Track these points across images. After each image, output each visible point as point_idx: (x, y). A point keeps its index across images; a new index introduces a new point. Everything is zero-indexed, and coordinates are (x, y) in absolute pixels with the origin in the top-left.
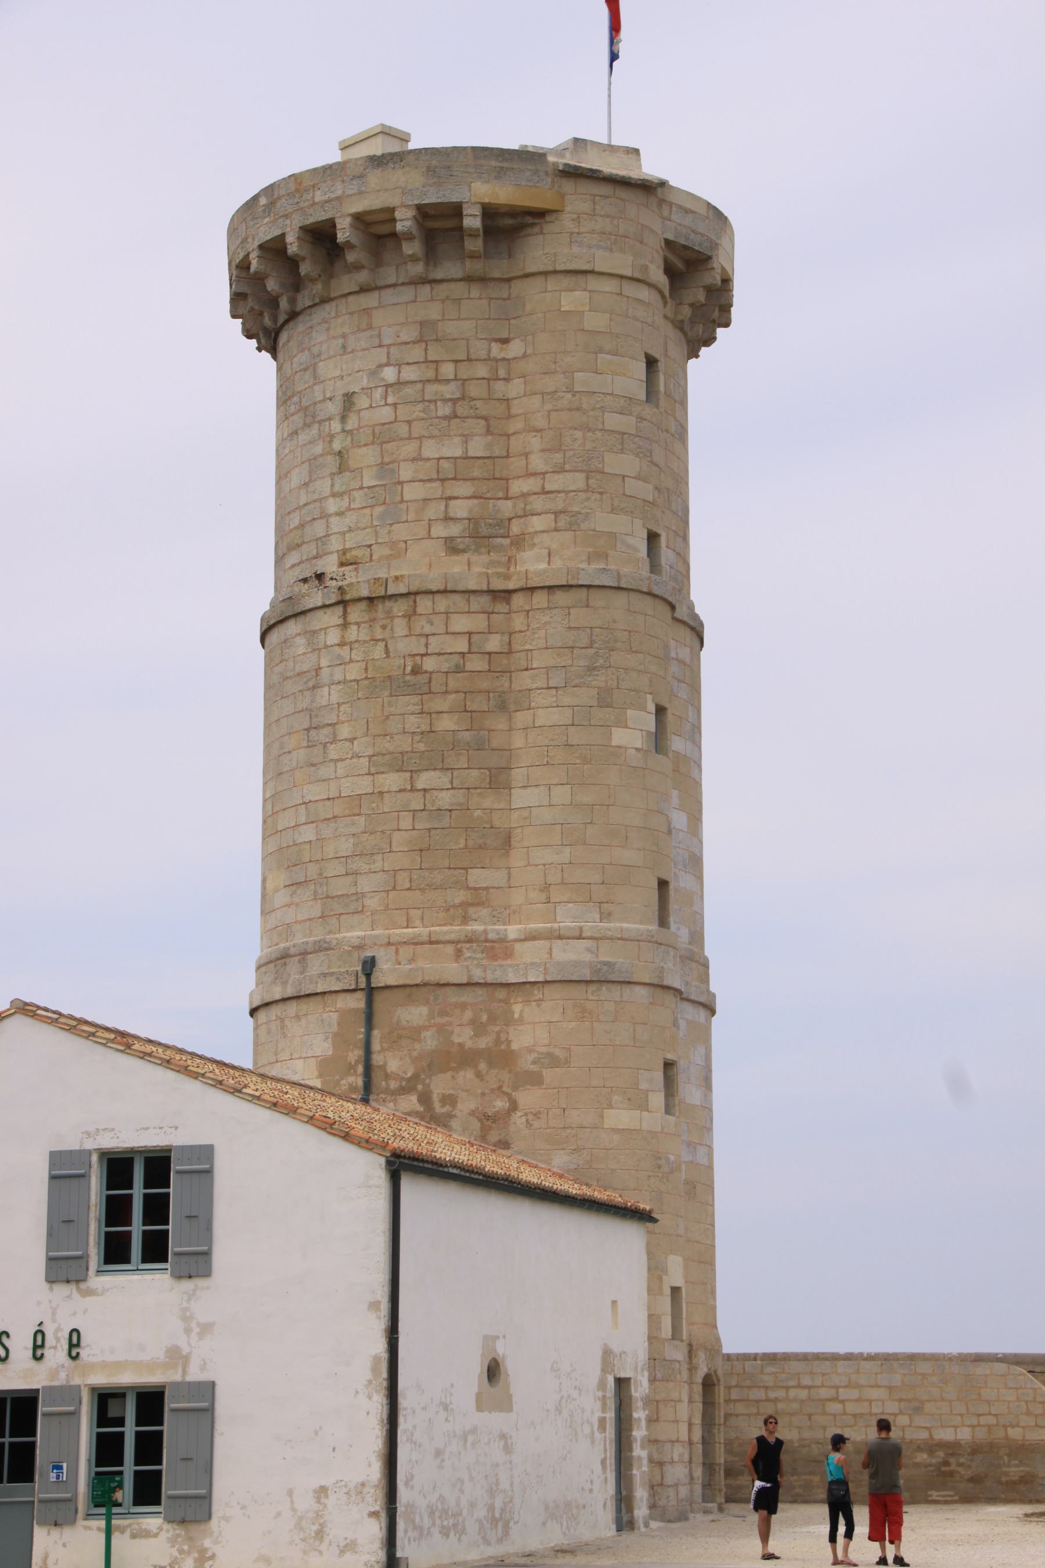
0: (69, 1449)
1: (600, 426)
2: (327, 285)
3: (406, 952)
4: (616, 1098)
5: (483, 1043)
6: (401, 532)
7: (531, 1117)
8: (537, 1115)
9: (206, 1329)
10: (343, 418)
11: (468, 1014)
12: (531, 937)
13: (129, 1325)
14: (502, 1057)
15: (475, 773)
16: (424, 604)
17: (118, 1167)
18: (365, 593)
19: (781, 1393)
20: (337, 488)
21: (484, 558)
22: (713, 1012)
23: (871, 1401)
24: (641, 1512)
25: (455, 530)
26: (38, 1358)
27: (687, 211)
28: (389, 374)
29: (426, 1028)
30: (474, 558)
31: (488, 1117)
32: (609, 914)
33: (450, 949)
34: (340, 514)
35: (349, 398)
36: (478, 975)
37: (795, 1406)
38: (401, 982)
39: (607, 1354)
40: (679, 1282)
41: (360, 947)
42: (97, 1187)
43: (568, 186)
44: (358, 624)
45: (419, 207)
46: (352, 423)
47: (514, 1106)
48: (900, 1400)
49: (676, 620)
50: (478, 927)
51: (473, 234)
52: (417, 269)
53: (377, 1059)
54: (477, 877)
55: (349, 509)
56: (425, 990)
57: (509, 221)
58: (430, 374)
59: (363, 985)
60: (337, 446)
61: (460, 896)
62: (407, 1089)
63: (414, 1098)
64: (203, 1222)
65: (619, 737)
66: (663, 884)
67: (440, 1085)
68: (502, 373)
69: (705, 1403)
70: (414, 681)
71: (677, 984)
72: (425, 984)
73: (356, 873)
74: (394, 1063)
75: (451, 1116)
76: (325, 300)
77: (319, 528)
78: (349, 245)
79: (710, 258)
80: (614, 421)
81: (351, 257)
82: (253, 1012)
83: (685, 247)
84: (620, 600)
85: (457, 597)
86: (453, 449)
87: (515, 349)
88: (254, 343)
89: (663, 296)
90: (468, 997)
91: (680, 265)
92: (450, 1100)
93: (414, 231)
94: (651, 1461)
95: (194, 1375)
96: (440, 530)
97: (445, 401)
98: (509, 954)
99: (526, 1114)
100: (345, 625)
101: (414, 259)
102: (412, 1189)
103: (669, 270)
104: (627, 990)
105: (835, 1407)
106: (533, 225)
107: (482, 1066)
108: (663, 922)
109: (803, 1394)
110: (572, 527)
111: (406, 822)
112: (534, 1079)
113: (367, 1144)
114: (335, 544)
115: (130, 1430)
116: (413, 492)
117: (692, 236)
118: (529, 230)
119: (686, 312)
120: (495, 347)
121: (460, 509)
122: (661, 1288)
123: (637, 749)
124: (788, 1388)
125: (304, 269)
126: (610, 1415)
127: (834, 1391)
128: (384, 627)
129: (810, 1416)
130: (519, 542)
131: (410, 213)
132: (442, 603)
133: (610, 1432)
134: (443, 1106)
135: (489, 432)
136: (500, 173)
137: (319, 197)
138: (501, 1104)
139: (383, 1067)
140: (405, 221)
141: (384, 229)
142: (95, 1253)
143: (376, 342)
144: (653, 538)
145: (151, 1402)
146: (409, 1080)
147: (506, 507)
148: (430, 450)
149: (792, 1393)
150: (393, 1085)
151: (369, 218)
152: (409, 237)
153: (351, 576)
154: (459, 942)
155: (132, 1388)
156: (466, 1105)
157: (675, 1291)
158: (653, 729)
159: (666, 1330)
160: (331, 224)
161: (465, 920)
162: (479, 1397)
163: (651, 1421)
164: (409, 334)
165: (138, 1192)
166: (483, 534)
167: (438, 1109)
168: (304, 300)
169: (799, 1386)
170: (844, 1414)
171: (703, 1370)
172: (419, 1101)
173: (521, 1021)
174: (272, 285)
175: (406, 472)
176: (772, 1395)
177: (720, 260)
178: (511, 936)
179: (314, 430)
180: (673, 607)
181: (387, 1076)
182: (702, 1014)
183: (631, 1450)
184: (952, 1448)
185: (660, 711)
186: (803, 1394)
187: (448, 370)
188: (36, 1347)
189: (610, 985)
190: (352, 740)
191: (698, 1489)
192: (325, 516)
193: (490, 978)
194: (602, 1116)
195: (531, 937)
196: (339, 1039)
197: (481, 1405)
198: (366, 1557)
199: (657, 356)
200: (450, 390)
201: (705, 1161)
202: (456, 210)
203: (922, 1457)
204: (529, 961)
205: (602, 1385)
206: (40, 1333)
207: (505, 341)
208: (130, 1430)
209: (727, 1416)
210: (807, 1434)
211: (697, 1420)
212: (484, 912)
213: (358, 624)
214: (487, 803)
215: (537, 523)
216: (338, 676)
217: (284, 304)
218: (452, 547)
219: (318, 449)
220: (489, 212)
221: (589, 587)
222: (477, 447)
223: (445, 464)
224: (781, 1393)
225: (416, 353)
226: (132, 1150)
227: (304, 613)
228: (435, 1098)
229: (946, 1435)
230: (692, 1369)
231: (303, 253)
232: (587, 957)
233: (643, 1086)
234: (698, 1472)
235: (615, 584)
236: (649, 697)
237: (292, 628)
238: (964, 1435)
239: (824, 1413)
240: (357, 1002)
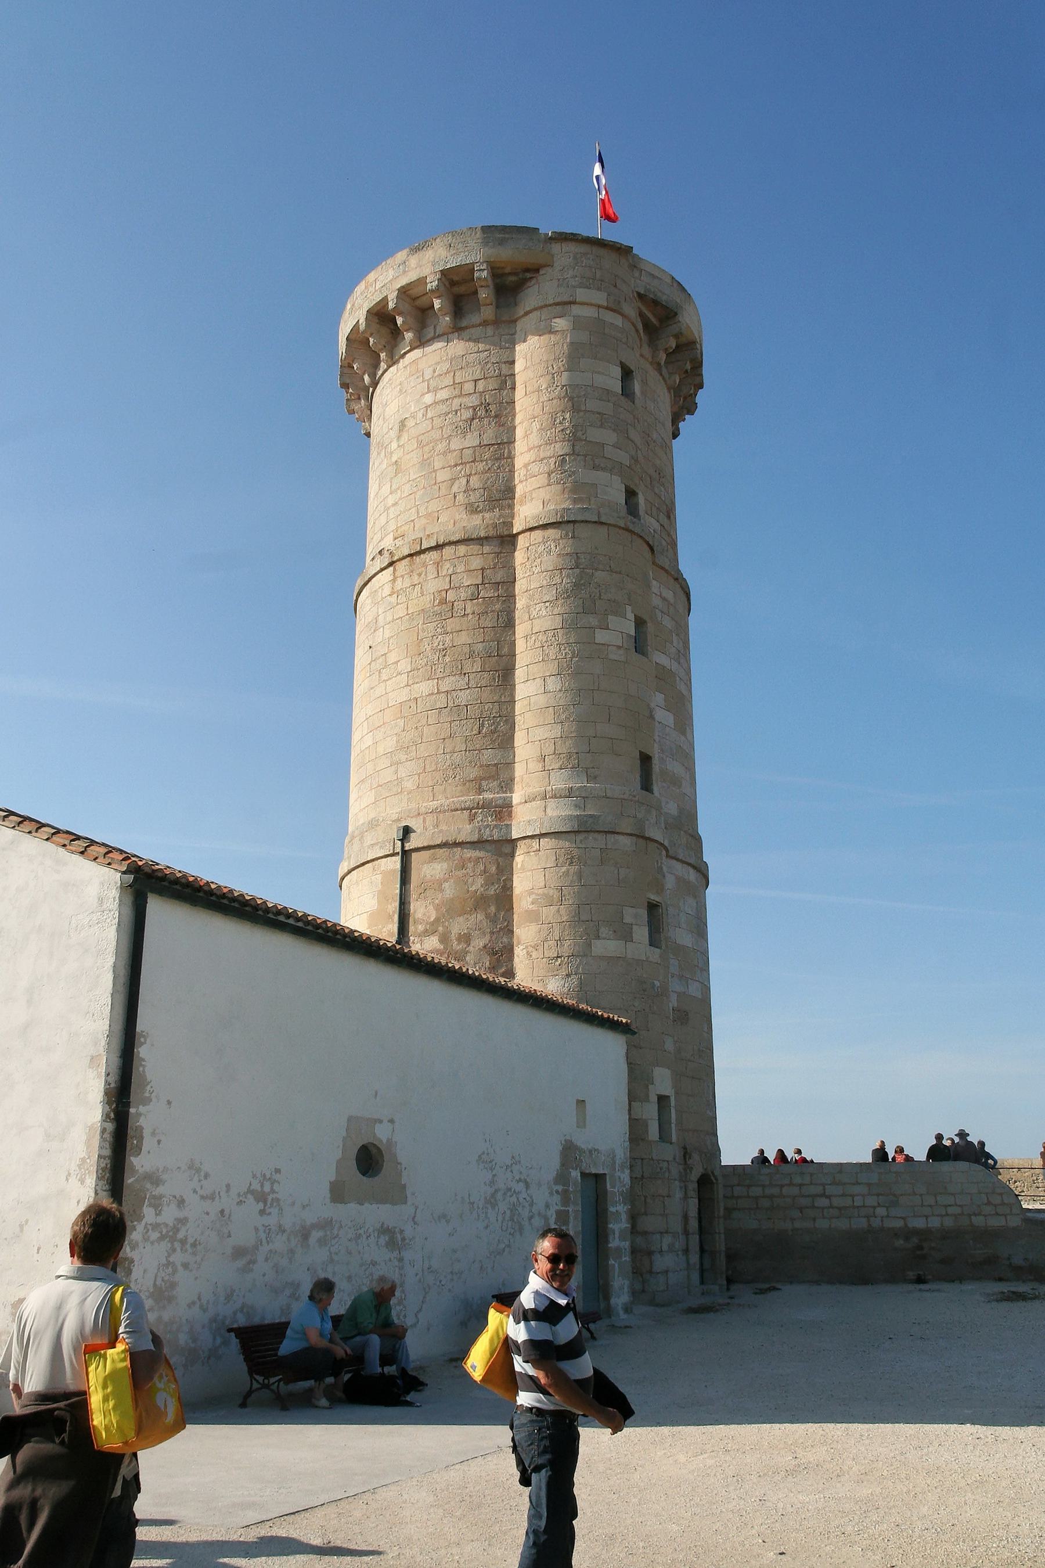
1: (583, 408)
4: (604, 931)
7: (530, 949)
10: (399, 438)
18: (406, 552)
23: (853, 1196)
24: (620, 1299)
27: (653, 276)
28: (428, 399)
29: (446, 880)
32: (595, 777)
34: (395, 504)
38: (426, 844)
40: (667, 1090)
43: (556, 248)
44: (402, 576)
48: (878, 1195)
49: (654, 563)
50: (488, 796)
55: (401, 499)
57: (513, 278)
59: (398, 849)
60: (394, 459)
66: (646, 760)
79: (676, 314)
94: (634, 1251)
99: (527, 947)
100: (394, 580)
104: (611, 838)
105: (823, 1202)
106: (531, 278)
117: (659, 294)
118: (529, 284)
119: (662, 357)
122: (647, 1096)
123: (619, 647)
124: (782, 1186)
127: (821, 1188)
128: (420, 575)
134: (458, 944)
136: (502, 242)
146: (432, 924)
149: (785, 1190)
150: (421, 928)
154: (473, 808)
158: (633, 633)
159: (653, 1131)
161: (480, 790)
169: (791, 1184)
170: (831, 1207)
172: (441, 941)
177: (686, 318)
182: (692, 876)
183: (607, 1242)
184: (924, 1234)
185: (640, 623)
186: (795, 1191)
189: (596, 835)
190: (397, 663)
194: (590, 945)
196: (382, 897)
197: (338, 1193)
199: (632, 368)
201: (694, 990)
203: (900, 1243)
205: (562, 1178)
209: (729, 1211)
210: (798, 1225)
211: (693, 1213)
213: (402, 576)
216: (389, 618)
224: (775, 1191)
228: (453, 937)
229: (919, 1223)
230: (687, 1168)
233: (628, 919)
234: (695, 1258)
235: (596, 519)
236: (629, 608)
238: (935, 1223)
239: (813, 1207)
240: (396, 863)
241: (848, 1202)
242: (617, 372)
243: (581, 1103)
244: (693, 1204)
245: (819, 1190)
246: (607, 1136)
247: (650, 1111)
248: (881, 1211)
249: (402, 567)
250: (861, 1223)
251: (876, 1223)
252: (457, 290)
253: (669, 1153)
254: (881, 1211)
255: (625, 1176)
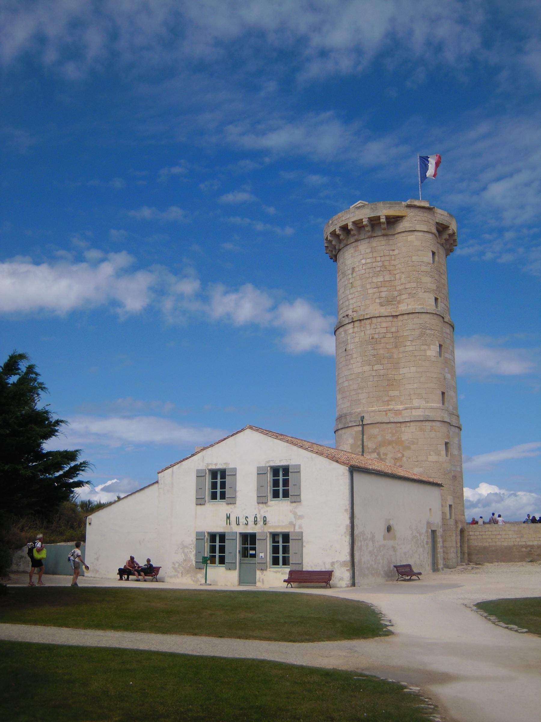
0: (264, 551)
2: (347, 240)
3: (372, 414)
4: (432, 453)
5: (394, 439)
6: (368, 302)
8: (409, 458)
9: (301, 517)
10: (352, 274)
11: (390, 431)
12: (406, 409)
13: (279, 515)
14: (399, 442)
15: (389, 365)
16: (374, 320)
17: (275, 471)
19: (483, 533)
20: (351, 292)
21: (390, 307)
22: (461, 430)
25: (382, 300)
26: (256, 524)
28: (363, 261)
30: (387, 307)
31: (396, 459)
33: (384, 413)
35: (353, 268)
36: (392, 420)
37: (488, 536)
39: (428, 523)
41: (360, 413)
42: (270, 477)
45: (369, 218)
46: (354, 275)
47: (403, 456)
50: (392, 407)
51: (383, 223)
52: (369, 234)
53: (365, 444)
54: (392, 393)
56: (377, 425)
58: (374, 260)
60: (351, 281)
61: (386, 399)
62: (374, 451)
63: (376, 454)
64: (298, 486)
65: (429, 353)
67: (383, 450)
68: (393, 258)
69: (461, 536)
70: (373, 341)
71: (448, 420)
72: (378, 423)
73: (359, 393)
74: (370, 444)
75: (386, 459)
76: (347, 245)
77: (347, 303)
78: (351, 230)
80: (423, 268)
81: (352, 233)
82: (335, 432)
83: (442, 224)
84: (428, 316)
85: (382, 318)
86: (381, 279)
87: (396, 252)
88: (332, 260)
89: (436, 236)
90: (389, 426)
91: (441, 229)
92: (386, 454)
93: (368, 224)
94: (444, 552)
95: (297, 529)
96: (378, 301)
97: (378, 267)
98: (400, 414)
100: (354, 327)
101: (368, 231)
102: (356, 476)
103: (438, 230)
105: (499, 537)
107: (394, 445)
108: (443, 404)
109: (490, 533)
110: (413, 297)
111: (371, 379)
112: (409, 448)
113: (344, 463)
114: (351, 307)
115: (281, 544)
116: (370, 291)
119: (444, 241)
120: (391, 252)
121: (383, 295)
125: (342, 237)
126: (430, 540)
129: (492, 539)
130: (399, 302)
131: (367, 220)
132: (379, 320)
133: (430, 545)
135: (390, 274)
137: (344, 219)
138: (399, 455)
139: (367, 446)
140: (365, 222)
141: (360, 225)
142: (270, 495)
143: (360, 253)
144: (436, 299)
145: (286, 537)
147: (396, 293)
148: (375, 280)
149: (487, 533)
150: (370, 450)
151: (358, 222)
152: (366, 226)
153: (355, 314)
155: (281, 533)
156: (390, 456)
157: (450, 506)
160: (347, 225)
161: (388, 405)
162: (384, 536)
163: (444, 542)
164: (368, 251)
165: (281, 478)
166: (389, 301)
167: (382, 457)
168: (342, 246)
171: (460, 527)
173: (404, 432)
174: (334, 243)
175: (368, 286)
176: (481, 534)
178: (401, 409)
179: (345, 278)
180: (443, 318)
181: (368, 448)
184: (532, 547)
185: (440, 346)
187: (378, 259)
188: (255, 521)
190: (356, 358)
191: (459, 559)
192: (348, 300)
193: (396, 420)
195: (406, 409)
198: (346, 582)
200: (380, 264)
201: (459, 469)
202: (379, 218)
204: (406, 416)
205: (427, 532)
206: (256, 517)
207: (394, 250)
208: (281, 544)
210: (490, 544)
211: (459, 540)
212: (394, 402)
214: (393, 373)
215: (404, 297)
217: (337, 247)
218: (381, 305)
219: (346, 283)
220: (388, 218)
221: (418, 313)
222: (387, 278)
223: (379, 283)
224: (483, 533)
225: (370, 255)
226: (279, 466)
227: (343, 325)
228: (381, 453)
231: (340, 233)
232: (422, 414)
234: (459, 555)
237: (341, 330)
238: (535, 543)
240: (360, 428)
241: (507, 537)
242: (431, 254)
243: (430, 509)
244: (459, 537)
245: (498, 533)
246: (437, 520)
247: (447, 509)
248: (518, 540)
249: (357, 324)
250: (511, 544)
251: (516, 543)
252: (372, 222)
253: (452, 522)
254: (518, 540)
255: (441, 530)
